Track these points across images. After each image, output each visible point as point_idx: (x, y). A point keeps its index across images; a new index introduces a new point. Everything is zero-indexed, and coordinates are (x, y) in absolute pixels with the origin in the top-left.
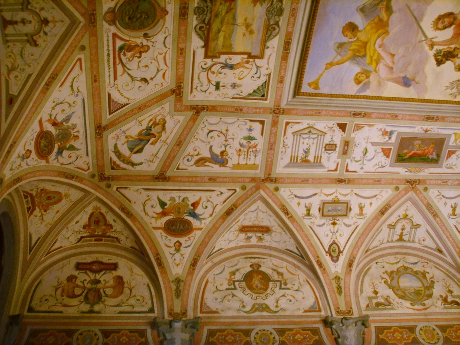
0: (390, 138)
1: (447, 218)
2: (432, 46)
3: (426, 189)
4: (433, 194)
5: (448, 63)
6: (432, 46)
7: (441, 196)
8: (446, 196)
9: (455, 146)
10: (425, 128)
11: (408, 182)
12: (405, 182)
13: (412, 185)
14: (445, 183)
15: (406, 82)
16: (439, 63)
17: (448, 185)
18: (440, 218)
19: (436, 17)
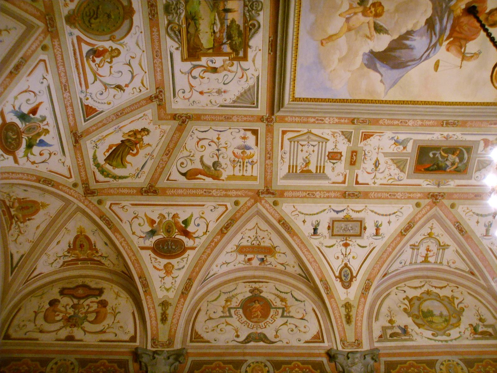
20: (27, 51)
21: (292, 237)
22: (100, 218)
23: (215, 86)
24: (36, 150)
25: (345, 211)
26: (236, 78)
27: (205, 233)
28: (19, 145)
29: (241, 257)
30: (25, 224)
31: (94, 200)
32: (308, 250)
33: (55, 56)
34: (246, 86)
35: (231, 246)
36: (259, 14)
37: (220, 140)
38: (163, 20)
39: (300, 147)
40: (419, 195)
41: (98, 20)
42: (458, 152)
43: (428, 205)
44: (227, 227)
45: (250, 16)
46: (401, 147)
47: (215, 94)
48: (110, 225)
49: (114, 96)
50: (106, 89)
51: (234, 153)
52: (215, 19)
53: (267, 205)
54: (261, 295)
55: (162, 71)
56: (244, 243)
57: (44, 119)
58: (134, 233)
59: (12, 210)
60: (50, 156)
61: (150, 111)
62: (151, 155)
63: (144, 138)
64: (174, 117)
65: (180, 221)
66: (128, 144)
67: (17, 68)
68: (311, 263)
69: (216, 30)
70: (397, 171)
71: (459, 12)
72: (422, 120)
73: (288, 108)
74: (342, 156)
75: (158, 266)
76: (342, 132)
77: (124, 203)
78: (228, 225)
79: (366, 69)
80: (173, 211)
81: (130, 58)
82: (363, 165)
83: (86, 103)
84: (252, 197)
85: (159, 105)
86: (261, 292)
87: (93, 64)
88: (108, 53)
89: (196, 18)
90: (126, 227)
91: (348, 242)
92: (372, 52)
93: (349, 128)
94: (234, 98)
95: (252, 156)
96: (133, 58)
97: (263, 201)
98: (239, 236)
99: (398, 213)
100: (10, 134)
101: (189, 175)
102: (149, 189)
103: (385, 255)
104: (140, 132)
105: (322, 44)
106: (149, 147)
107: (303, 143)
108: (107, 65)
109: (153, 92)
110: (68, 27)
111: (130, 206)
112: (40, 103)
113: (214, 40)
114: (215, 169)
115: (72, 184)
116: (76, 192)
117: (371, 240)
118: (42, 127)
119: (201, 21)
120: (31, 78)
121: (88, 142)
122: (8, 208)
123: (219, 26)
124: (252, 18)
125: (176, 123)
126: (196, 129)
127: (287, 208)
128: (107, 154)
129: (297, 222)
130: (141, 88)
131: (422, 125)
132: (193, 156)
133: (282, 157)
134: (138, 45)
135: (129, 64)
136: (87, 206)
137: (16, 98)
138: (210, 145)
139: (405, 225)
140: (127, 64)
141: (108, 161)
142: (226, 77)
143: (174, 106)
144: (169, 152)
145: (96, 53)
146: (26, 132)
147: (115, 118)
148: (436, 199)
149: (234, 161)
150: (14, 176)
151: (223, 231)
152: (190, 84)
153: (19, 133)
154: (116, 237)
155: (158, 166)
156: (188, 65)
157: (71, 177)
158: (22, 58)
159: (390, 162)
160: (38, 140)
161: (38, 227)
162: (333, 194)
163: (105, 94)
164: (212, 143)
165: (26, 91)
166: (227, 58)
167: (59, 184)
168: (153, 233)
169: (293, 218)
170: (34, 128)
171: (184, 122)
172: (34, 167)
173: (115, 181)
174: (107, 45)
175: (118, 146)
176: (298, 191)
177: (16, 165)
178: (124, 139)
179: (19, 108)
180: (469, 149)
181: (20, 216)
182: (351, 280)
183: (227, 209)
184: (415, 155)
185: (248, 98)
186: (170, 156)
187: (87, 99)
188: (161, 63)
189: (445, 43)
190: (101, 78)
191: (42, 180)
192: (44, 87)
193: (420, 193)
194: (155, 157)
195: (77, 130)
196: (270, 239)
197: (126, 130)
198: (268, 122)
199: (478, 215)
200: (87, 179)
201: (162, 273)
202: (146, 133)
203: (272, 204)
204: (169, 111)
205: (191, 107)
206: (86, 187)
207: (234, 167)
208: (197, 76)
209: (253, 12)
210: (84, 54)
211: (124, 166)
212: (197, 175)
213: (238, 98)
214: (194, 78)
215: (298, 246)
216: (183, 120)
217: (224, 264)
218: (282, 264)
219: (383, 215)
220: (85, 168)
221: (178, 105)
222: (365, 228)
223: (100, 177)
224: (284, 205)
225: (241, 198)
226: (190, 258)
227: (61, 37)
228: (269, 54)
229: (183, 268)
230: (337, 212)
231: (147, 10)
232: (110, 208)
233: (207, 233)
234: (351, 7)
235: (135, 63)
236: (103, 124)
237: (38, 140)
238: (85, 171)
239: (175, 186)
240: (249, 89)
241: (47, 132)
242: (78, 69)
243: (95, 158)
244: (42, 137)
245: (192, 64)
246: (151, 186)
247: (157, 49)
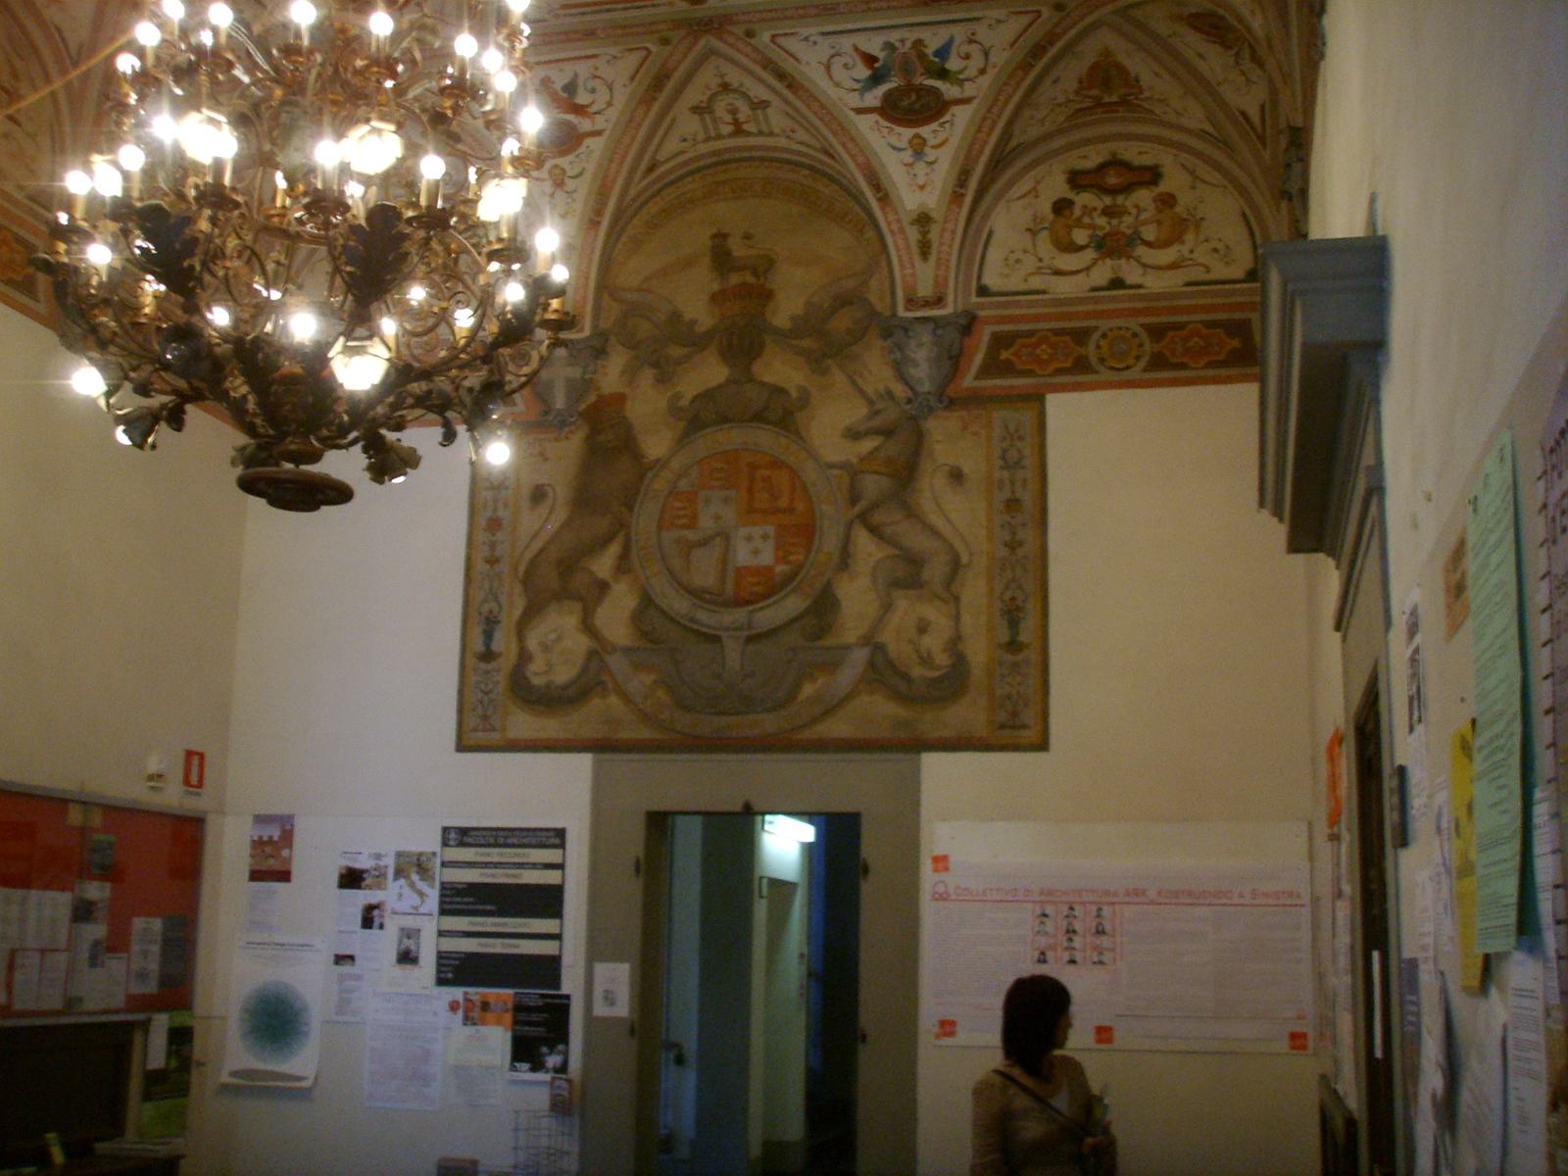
24: (953, 64)
28: (935, 92)
57: (889, 47)
59: (1107, 99)
60: (976, 42)
67: (781, 75)
100: (905, 103)
112: (856, 49)
116: (1076, 8)
122: (1099, 104)
150: (995, 110)
153: (909, 88)
157: (1039, 12)
161: (1157, 75)
165: (828, 68)
172: (991, 73)
177: (975, 103)
181: (1123, 91)
191: (1030, 60)
237: (932, 58)
241: (918, 44)
244: (929, 51)
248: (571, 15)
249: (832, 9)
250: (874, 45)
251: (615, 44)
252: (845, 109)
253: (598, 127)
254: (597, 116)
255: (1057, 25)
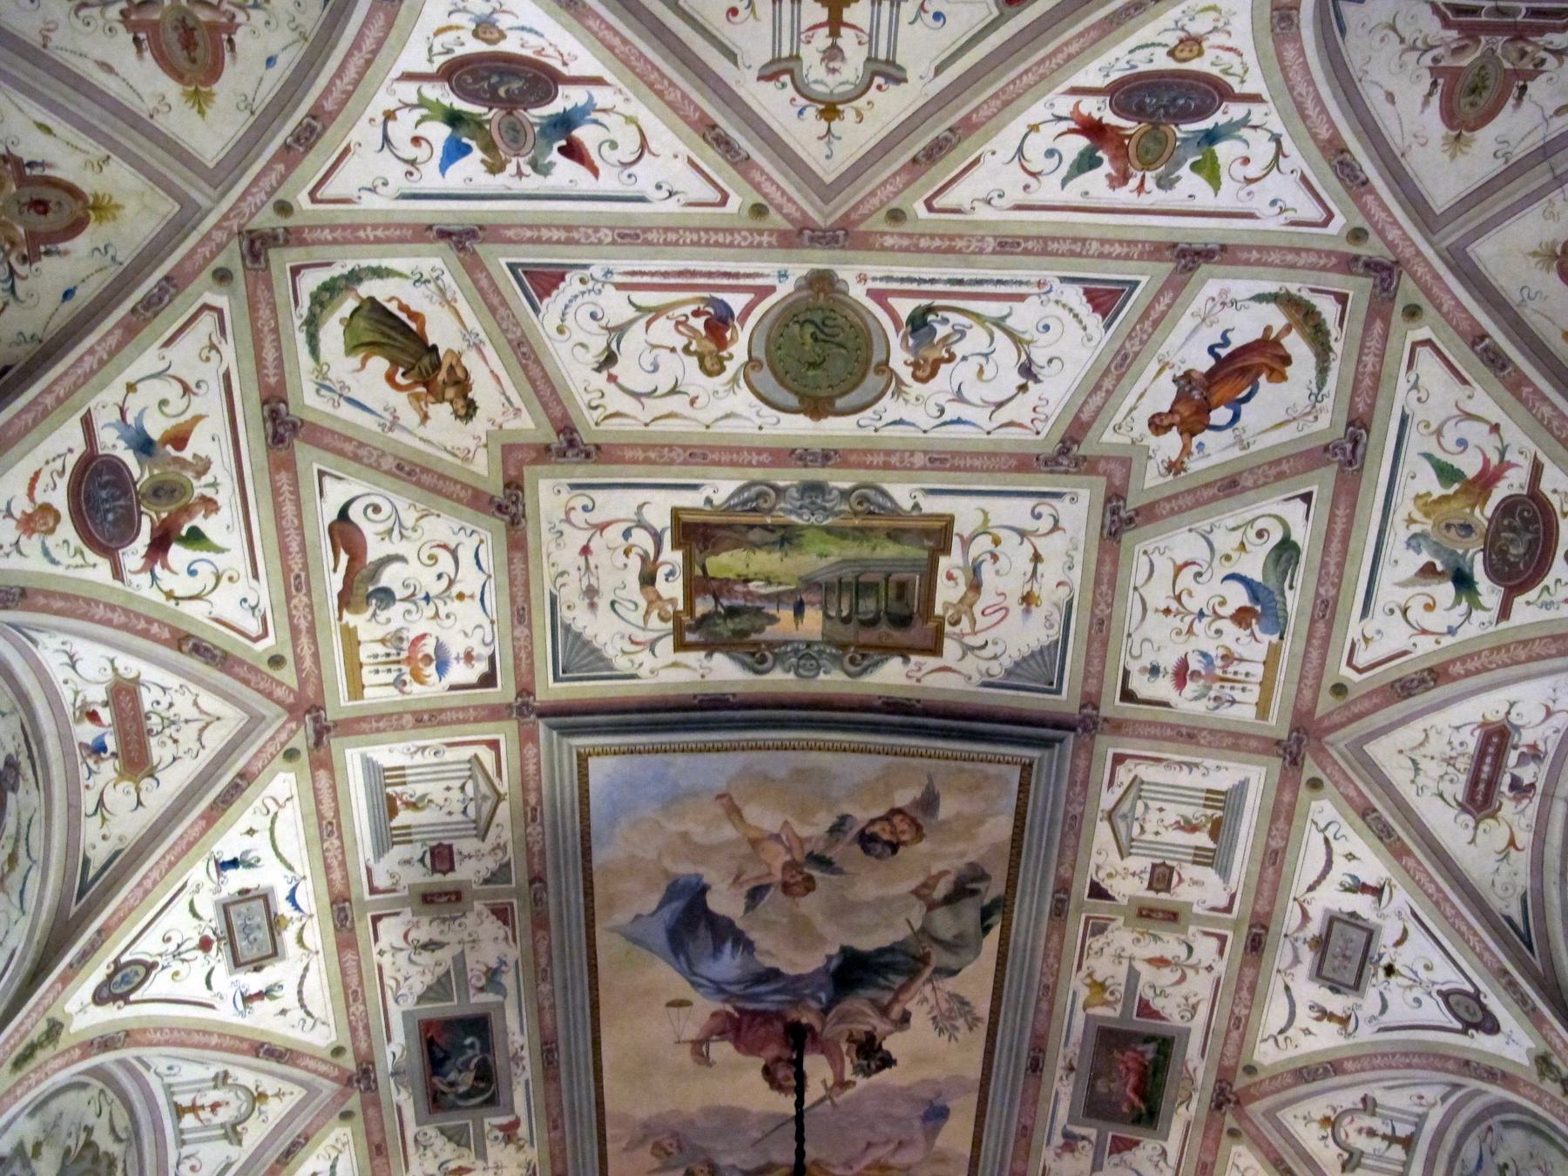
0: (1084, 1138)
1: (1351, 1041)
2: (851, 1084)
3: (1250, 1070)
4: (1266, 1054)
5: (886, 1046)
6: (842, 1084)
7: (1281, 1038)
8: (1282, 1023)
9: (1124, 1005)
10: (1059, 1072)
11: (1219, 1106)
12: (1218, 1115)
13: (1229, 1101)
14: (1240, 1025)
15: (937, 1114)
16: (887, 1061)
17: (1247, 1017)
18: (1348, 1059)
19: (775, 1094)
20: (763, 172)
21: (202, 816)
22: (167, 278)
23: (607, 585)
24: (439, 133)
25: (296, 914)
26: (630, 630)
27: (170, 595)
29: (97, 694)
30: (120, 28)
31: (232, 257)
32: (172, 865)
33: (731, 231)
34: (609, 652)
35: (130, 666)
36: (788, 671)
37: (457, 602)
38: (787, 478)
39: (458, 783)
40: (363, 1046)
41: (809, 340)
42: (482, 1085)
43: (342, 1070)
44: (200, 650)
45: (786, 653)
46: (483, 982)
47: (585, 583)
48: (146, 308)
49: (583, 345)
50: (607, 328)
51: (423, 636)
52: (780, 584)
53: (283, 736)
54: (10, 795)
55: (648, 461)
56: (147, 699)
58: (131, 388)
60: (406, 161)
61: (528, 424)
62: (394, 423)
63: (447, 407)
64: (514, 485)
65: (198, 521)
66: (426, 361)
67: (723, 144)
68: (139, 884)
69: (752, 586)
70: (419, 989)
71: (793, 1015)
72: (553, 1006)
73: (560, 745)
74: (445, 873)
75: (40, 486)
76: (508, 864)
77: (228, 350)
78: (207, 649)
79: (664, 887)
80: (226, 496)
81: (692, 394)
82: (425, 920)
83: (572, 278)
84: (300, 695)
85: (548, 448)
86: (14, 789)
87: (688, 309)
88: (712, 346)
89: (786, 545)
90: (147, 361)
91: (215, 946)
92: (704, 889)
93: (518, 876)
94: (577, 626)
95: (418, 678)
96: (692, 402)
97: (293, 725)
98: (172, 681)
99: (310, 1021)
100: (516, 85)
101: (344, 531)
102: (284, 423)
103: (197, 1038)
104: (465, 397)
105: (720, 797)
106: (416, 418)
107: (470, 788)
108: (680, 342)
109: (586, 438)
110: (804, 272)
111: (222, 371)
112: (595, 172)
113: (728, 580)
114: (369, 596)
115: (289, 199)
116: (258, 209)
117: (229, 993)
118: (514, 160)
119: (777, 555)
120: (681, 166)
121: (438, 262)
123: (763, 591)
124: (778, 658)
125: (495, 488)
126: (482, 541)
127: (283, 783)
128: (392, 307)
129: (248, 814)
130: (600, 410)
131: (540, 1009)
132: (402, 536)
133: (424, 749)
134: (727, 416)
135: (674, 391)
136: (207, 237)
137: (630, 120)
138: (440, 576)
139: (279, 1044)
140: (676, 385)
141: (367, 307)
142: (632, 606)
143: (545, 486)
144: (414, 474)
145: (719, 324)
146: (511, 119)
147: (510, 336)
148: (358, 1081)
149: (401, 639)
151: (187, 642)
152: (608, 524)
153: (511, 104)
154: (109, 333)
155: (361, 445)
156: (660, 519)
158: (748, 158)
159: (440, 970)
160: (473, 144)
161: (107, 68)
162: (337, 875)
163: (594, 326)
164: (445, 582)
165: (644, 145)
166: (680, 607)
167: (291, 166)
168: (144, 446)
169: (257, 803)
170: (515, 140)
171: (500, 508)
173: (298, 322)
174: (738, 351)
175: (419, 339)
176: (335, 799)
177: (396, 72)
178: (441, 353)
179: (596, 122)
180: (492, 1102)
182: (114, 998)
183: (256, 640)
184: (467, 1011)
185: (579, 655)
186: (397, 477)
187: (582, 281)
188: (671, 463)
189: (729, 1008)
190: (643, 322)
191: (318, 125)
192: (645, 186)
193: (370, 1047)
194: (390, 434)
195: (484, 241)
196: (175, 759)
197: (471, 361)
198: (519, 708)
199: (333, 1167)
200: (302, 243)
201: (22, 506)
202: (462, 412)
203: (287, 747)
204: (528, 471)
205: (544, 526)
206: (275, 238)
207: (383, 641)
208: (631, 541)
209: (794, 660)
210: (719, 296)
211: (351, 350)
212: (347, 551)
213: (578, 636)
214: (627, 534)
215: (181, 837)
216: (507, 507)
217: (71, 657)
218: (101, 803)
219: (300, 992)
220: (346, 242)
221: (549, 494)
222: (257, 969)
223: (311, 282)
224: (292, 776)
225: (293, 669)
226: (88, 574)
227: (781, 252)
228: (695, 696)
229: (54, 562)
230: (292, 898)
231: (817, 448)
232: (206, 307)
233: (172, 603)
234: (802, 841)
235: (677, 403)
236: (492, 302)
237: (473, 144)
238: (335, 242)
239: (303, 493)
240: (602, 659)
241: (495, 168)
242: (680, 274)
243: (379, 273)
244: (477, 154)
245: (664, 530)
246: (294, 428)
247: (710, 456)
248: (1020, 283)
249: (622, 236)
250: (565, 172)
251: (977, 224)
252: (620, 85)
253: (1073, 99)
254: (1065, 112)
255: (283, 179)
